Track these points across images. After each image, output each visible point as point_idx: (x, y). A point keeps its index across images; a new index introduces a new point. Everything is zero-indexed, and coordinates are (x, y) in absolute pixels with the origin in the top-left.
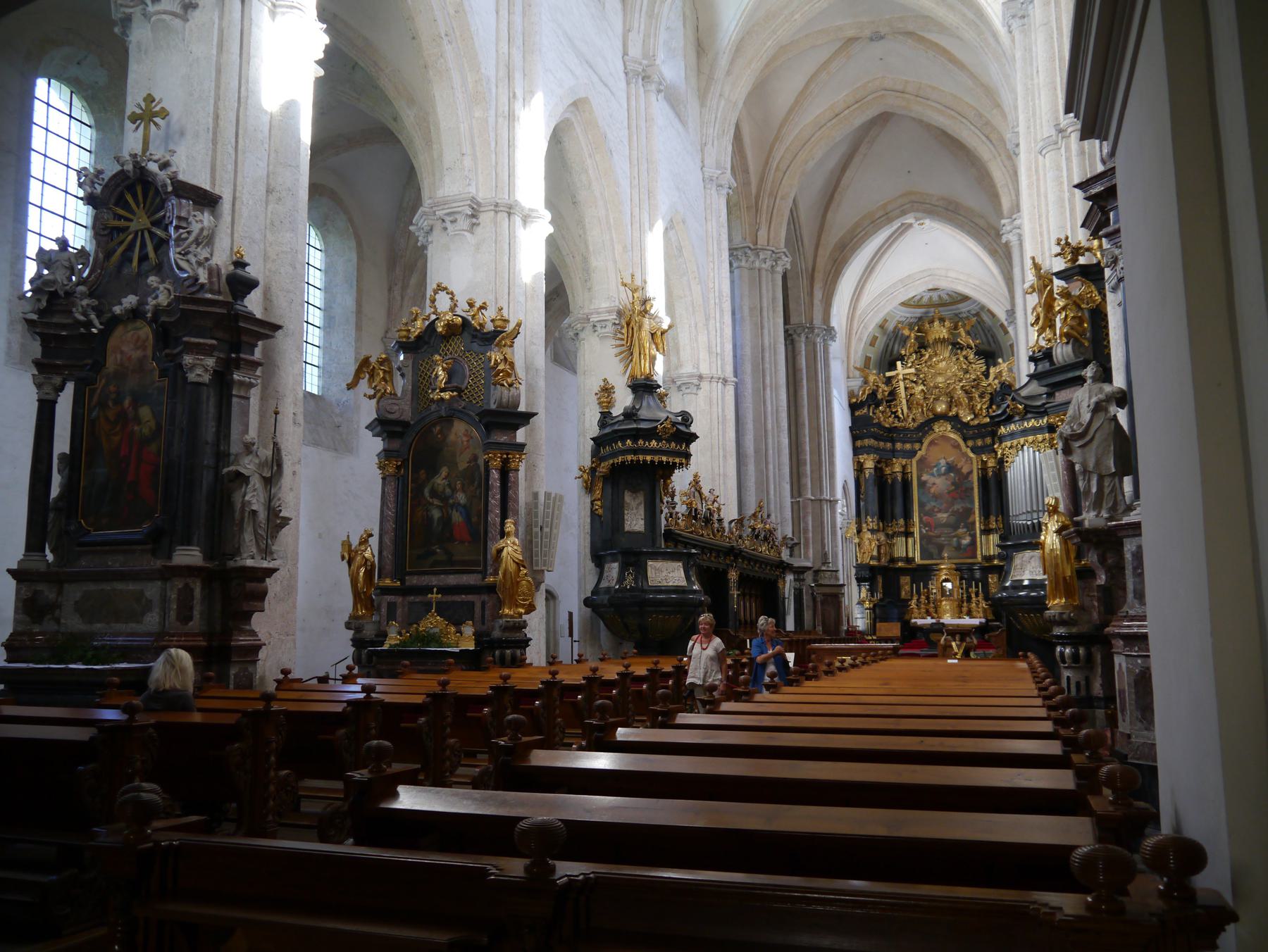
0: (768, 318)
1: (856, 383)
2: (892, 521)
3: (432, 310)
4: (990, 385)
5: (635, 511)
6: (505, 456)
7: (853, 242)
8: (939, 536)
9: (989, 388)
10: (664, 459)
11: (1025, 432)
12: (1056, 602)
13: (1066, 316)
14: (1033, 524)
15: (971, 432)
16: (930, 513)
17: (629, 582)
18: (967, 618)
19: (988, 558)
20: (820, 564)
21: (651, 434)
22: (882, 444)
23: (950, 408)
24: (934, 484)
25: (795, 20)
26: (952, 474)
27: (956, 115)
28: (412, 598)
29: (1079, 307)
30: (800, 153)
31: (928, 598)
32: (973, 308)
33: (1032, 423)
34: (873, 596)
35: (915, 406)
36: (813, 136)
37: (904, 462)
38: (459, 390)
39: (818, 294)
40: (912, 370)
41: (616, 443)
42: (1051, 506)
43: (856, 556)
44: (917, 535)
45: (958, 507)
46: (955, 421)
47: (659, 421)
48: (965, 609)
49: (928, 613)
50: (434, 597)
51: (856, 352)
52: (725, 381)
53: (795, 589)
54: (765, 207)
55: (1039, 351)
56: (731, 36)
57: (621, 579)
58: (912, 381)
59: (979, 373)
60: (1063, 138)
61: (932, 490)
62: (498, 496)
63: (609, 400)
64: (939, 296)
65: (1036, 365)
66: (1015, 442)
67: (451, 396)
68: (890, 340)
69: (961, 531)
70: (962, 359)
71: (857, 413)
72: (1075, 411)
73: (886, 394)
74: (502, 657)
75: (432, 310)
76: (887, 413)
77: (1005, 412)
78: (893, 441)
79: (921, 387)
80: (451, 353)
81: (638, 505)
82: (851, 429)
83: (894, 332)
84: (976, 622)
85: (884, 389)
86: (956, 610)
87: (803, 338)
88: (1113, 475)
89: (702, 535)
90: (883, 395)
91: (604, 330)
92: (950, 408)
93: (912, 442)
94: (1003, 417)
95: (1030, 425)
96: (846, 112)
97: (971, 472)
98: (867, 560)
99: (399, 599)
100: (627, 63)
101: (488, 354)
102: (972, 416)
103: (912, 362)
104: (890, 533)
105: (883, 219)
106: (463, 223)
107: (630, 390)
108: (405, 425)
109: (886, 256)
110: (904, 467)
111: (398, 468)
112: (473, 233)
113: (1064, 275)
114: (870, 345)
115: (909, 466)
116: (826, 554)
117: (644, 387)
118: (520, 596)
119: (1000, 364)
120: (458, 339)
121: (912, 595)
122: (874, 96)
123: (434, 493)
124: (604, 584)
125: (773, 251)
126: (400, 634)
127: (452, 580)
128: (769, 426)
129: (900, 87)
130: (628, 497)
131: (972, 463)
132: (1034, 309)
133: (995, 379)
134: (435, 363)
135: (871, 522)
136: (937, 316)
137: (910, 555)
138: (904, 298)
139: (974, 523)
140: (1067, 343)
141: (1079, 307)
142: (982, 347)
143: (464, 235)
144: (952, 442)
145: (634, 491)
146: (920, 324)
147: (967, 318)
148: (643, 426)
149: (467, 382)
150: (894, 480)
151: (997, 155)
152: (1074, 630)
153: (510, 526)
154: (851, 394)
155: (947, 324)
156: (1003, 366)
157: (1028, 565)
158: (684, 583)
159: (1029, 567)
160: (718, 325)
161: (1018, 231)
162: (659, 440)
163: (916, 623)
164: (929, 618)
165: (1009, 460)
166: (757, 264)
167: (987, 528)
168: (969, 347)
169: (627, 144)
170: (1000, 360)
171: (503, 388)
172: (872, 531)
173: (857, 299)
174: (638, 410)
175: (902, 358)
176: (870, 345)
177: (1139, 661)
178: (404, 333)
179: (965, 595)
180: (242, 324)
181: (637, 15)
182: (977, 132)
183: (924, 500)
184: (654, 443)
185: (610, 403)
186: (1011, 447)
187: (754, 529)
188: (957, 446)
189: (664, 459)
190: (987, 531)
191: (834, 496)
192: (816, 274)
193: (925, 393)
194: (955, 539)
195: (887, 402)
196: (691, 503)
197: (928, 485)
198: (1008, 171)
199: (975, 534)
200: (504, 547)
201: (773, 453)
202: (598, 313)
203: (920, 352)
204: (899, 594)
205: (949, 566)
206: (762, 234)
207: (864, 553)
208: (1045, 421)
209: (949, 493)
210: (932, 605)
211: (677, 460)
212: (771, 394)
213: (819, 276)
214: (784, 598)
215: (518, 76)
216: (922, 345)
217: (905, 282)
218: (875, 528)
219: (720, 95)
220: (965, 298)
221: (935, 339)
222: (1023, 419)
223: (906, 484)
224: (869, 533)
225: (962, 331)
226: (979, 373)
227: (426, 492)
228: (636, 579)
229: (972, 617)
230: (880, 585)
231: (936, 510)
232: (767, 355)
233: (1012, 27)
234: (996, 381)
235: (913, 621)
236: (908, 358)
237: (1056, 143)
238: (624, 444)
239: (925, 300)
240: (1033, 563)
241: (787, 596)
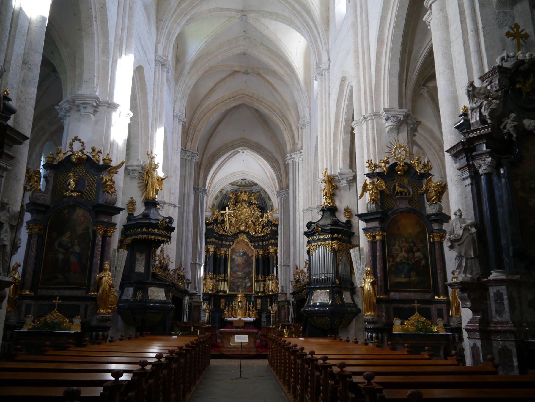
0: (188, 181)
1: (209, 214)
2: (219, 274)
3: (70, 149)
4: (263, 221)
5: (140, 262)
6: (106, 229)
7: (218, 155)
8: (238, 282)
9: (262, 222)
10: (160, 238)
11: (320, 240)
12: (369, 313)
13: (373, 192)
14: (322, 278)
15: (254, 239)
16: (235, 272)
17: (139, 297)
18: (248, 318)
19: (257, 293)
21: (155, 226)
22: (217, 241)
23: (246, 229)
24: (237, 260)
25: (219, 58)
26: (245, 256)
27: (272, 110)
28: (41, 302)
29: (377, 189)
30: (208, 114)
31: (232, 309)
32: (258, 189)
33: (324, 236)
34: (210, 307)
36: (214, 107)
37: (226, 249)
38: (82, 193)
39: (202, 174)
40: (232, 211)
41: (137, 229)
42: (368, 271)
43: (204, 289)
44: (229, 281)
45: (246, 270)
46: (248, 234)
47: (160, 220)
48: (247, 314)
49: (232, 315)
50: (57, 302)
51: (210, 201)
52: (175, 206)
53: (189, 303)
54: (191, 134)
55: (326, 207)
56: (193, 57)
57: (135, 295)
58: (232, 216)
60: (365, 121)
61: (236, 262)
62: (100, 250)
63: (133, 208)
64: (245, 182)
65: (323, 213)
66: (316, 244)
67: (77, 195)
69: (247, 280)
70: (252, 209)
72: (451, 229)
73: (221, 220)
74: (97, 336)
75: (70, 149)
76: (220, 228)
77: (312, 230)
78: (222, 240)
79: (235, 219)
80: (78, 173)
81: (142, 259)
83: (225, 194)
84: (252, 319)
85: (220, 218)
86: (244, 314)
88: (472, 258)
89: (163, 276)
90: (220, 221)
91: (133, 175)
92: (246, 229)
93: (230, 242)
94: (312, 233)
95: (323, 237)
96: (228, 100)
97: (253, 256)
98: (208, 291)
99: (33, 302)
100: (157, 57)
101: (101, 176)
102: (255, 233)
103: (232, 208)
104: (218, 279)
105: (231, 147)
106: (91, 110)
107: (144, 204)
108: (47, 207)
109: (227, 163)
110: (225, 252)
111: (40, 230)
112: (94, 115)
113: (370, 175)
114: (215, 199)
117: (150, 204)
118: (109, 303)
119: (268, 212)
120: (83, 166)
122: (240, 96)
123: (60, 245)
124: (123, 298)
125: (192, 153)
126: (34, 322)
127: (68, 293)
128: (184, 228)
129: (251, 95)
130: (138, 256)
131: (253, 252)
132: (324, 189)
133: (265, 218)
134: (70, 177)
135: (211, 274)
136: (243, 190)
137: (225, 290)
138: (231, 181)
139: (252, 277)
140: (373, 203)
141: (377, 189)
142: (261, 205)
143: (90, 115)
145: (141, 253)
146: (236, 193)
147: (255, 193)
148: (152, 221)
149: (86, 189)
150: (221, 257)
151: (286, 129)
152: (377, 326)
153: (107, 265)
154: (207, 219)
155: (247, 194)
156: (269, 214)
157: (320, 297)
158: (164, 299)
159: (320, 298)
160: (174, 180)
161: (293, 160)
162: (159, 229)
163: (227, 319)
164: (232, 317)
165: (313, 251)
166: (185, 157)
167: (257, 280)
169: (153, 91)
170: (268, 211)
171: (109, 194)
172: (211, 279)
173: (213, 179)
174: (149, 214)
175: (228, 206)
176: (215, 199)
177: (501, 343)
178: (51, 159)
179: (248, 308)
180: (8, 132)
181: (163, 37)
182: (280, 118)
184: (156, 230)
185: (134, 210)
186: (314, 246)
187: (179, 275)
188: (248, 245)
189: (160, 238)
190: (257, 281)
191: (201, 262)
192: (202, 166)
193: (236, 222)
194: (244, 284)
195: (221, 223)
196: (161, 261)
198: (290, 136)
199: (252, 282)
200: (103, 277)
201: (185, 241)
202: (132, 166)
203: (236, 204)
204: (220, 306)
205: (242, 295)
206: (189, 144)
207: (207, 288)
208: (329, 236)
209: (243, 264)
210: (234, 312)
211: (166, 240)
212: (186, 214)
213: (203, 167)
214: (184, 307)
215: (124, 46)
216: (237, 201)
217: (233, 174)
218: (212, 277)
219: (184, 82)
220: (256, 184)
221: (242, 200)
222: (319, 235)
223: (226, 259)
224: (210, 279)
225: (253, 197)
226: (258, 216)
227: (56, 244)
228: (142, 296)
229: (250, 317)
230: (213, 302)
231: (237, 271)
232: (186, 197)
233: (317, 78)
234: (266, 219)
235: (226, 318)
236: (231, 206)
237: (361, 123)
238: (141, 229)
239: (239, 183)
240: (322, 296)
241: (185, 306)
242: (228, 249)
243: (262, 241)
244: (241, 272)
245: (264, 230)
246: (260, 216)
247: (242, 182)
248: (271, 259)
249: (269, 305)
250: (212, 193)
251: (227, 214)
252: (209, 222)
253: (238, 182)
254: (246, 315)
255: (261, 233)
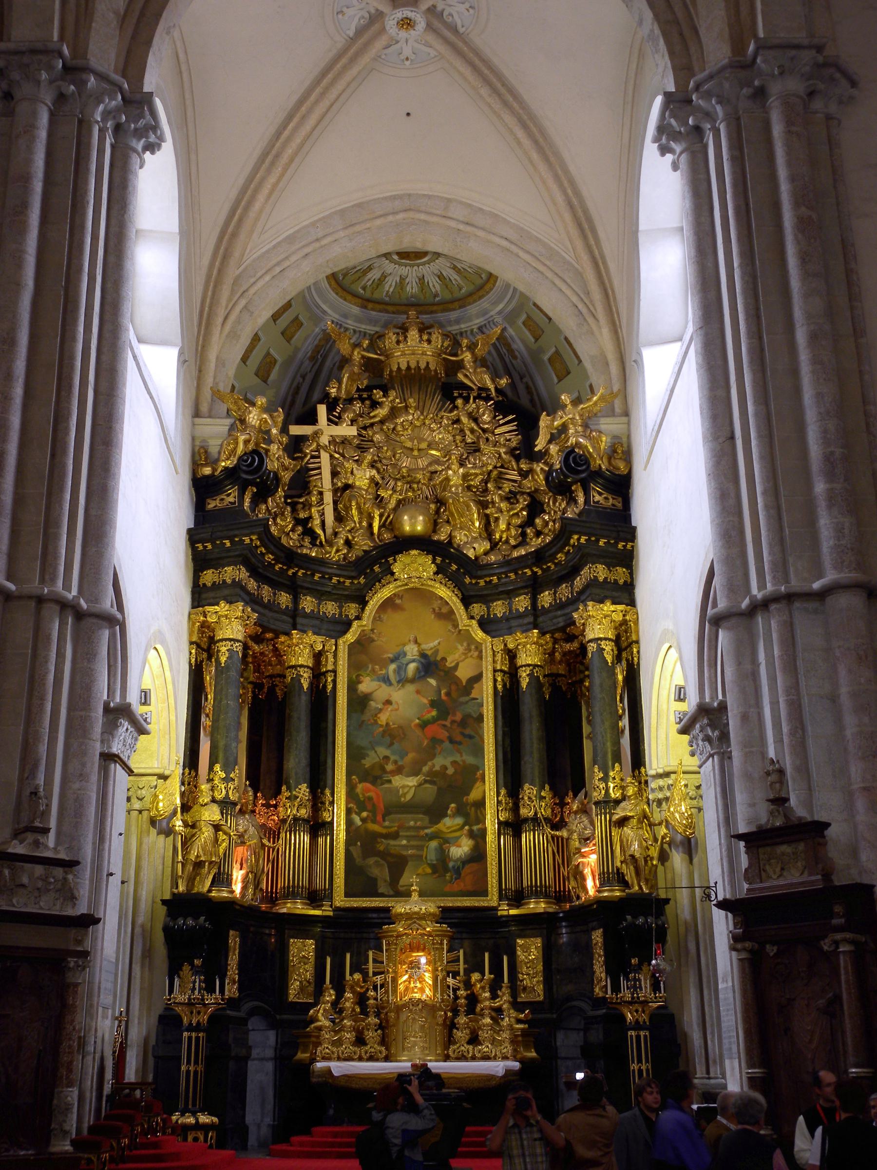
8: (395, 836)
15: (482, 583)
16: (376, 776)
20: (7, 832)
22: (266, 592)
23: (435, 526)
24: (388, 702)
26: (433, 682)
31: (362, 999)
35: (354, 512)
37: (318, 642)
51: (221, 362)
59: (502, 450)
61: (383, 718)
64: (422, 279)
68: (304, 377)
69: (450, 823)
70: (464, 420)
71: (212, 504)
82: (193, 537)
87: (48, 97)
93: (342, 598)
97: (478, 678)
110: (318, 656)
115: (331, 659)
116: (35, 793)
121: (319, 992)
131: (480, 657)
144: (436, 605)
156: (569, 415)
168: (483, 394)
172: (225, 805)
183: (362, 741)
188: (448, 616)
194: (434, 844)
197: (372, 703)
199: (484, 831)
203: (370, 398)
209: (424, 725)
221: (409, 368)
224: (215, 808)
225: (467, 357)
231: (390, 767)
234: (553, 449)
239: (389, 286)
242: (330, 644)
243: (535, 587)
244: (416, 774)
245: (538, 521)
246: (511, 452)
247: (402, 279)
248: (596, 682)
249: (599, 969)
250: (232, 318)
251: (324, 440)
252: (214, 470)
253: (384, 276)
254: (450, 1040)
255: (523, 543)
